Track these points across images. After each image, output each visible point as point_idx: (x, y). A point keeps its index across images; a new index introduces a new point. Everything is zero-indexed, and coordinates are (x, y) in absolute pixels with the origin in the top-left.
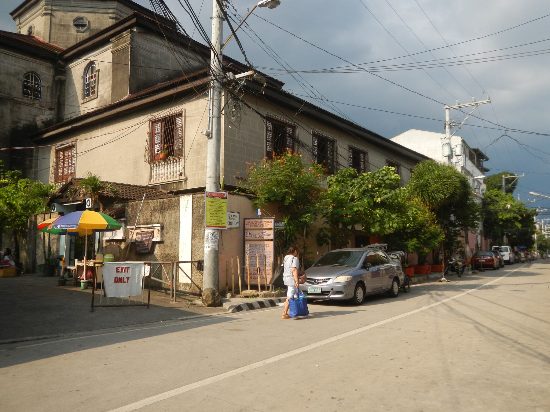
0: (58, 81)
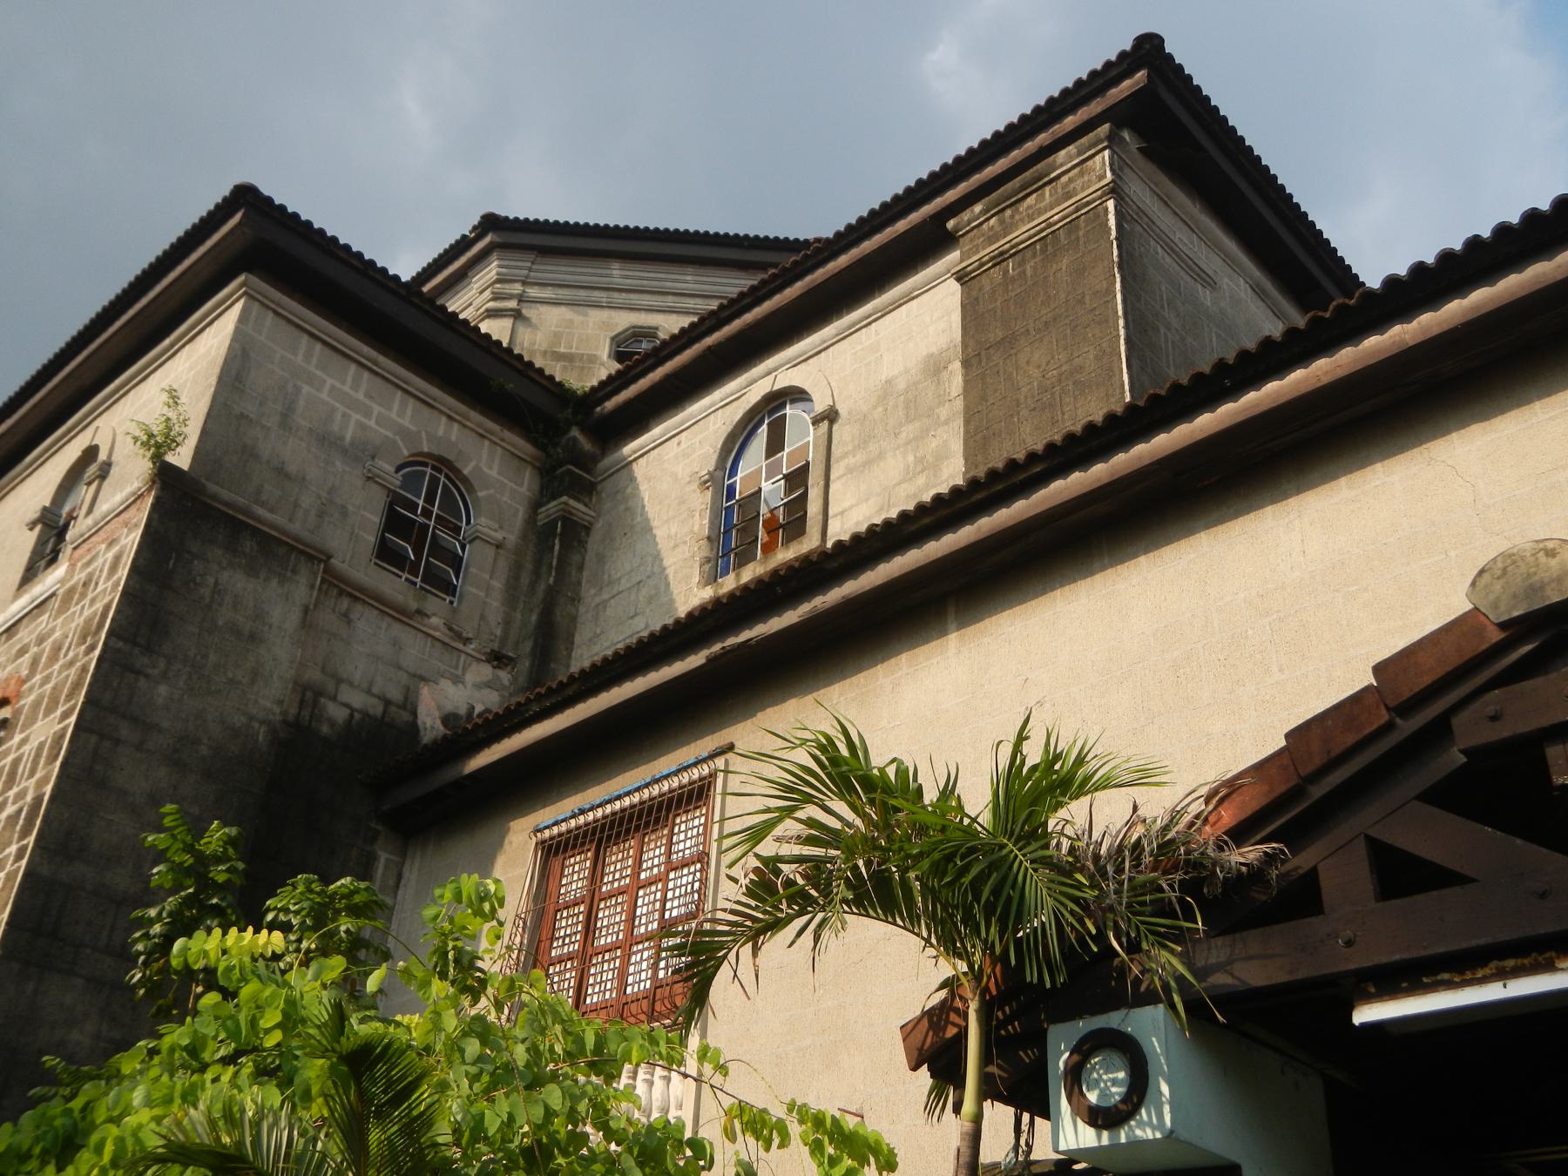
0: (553, 523)
